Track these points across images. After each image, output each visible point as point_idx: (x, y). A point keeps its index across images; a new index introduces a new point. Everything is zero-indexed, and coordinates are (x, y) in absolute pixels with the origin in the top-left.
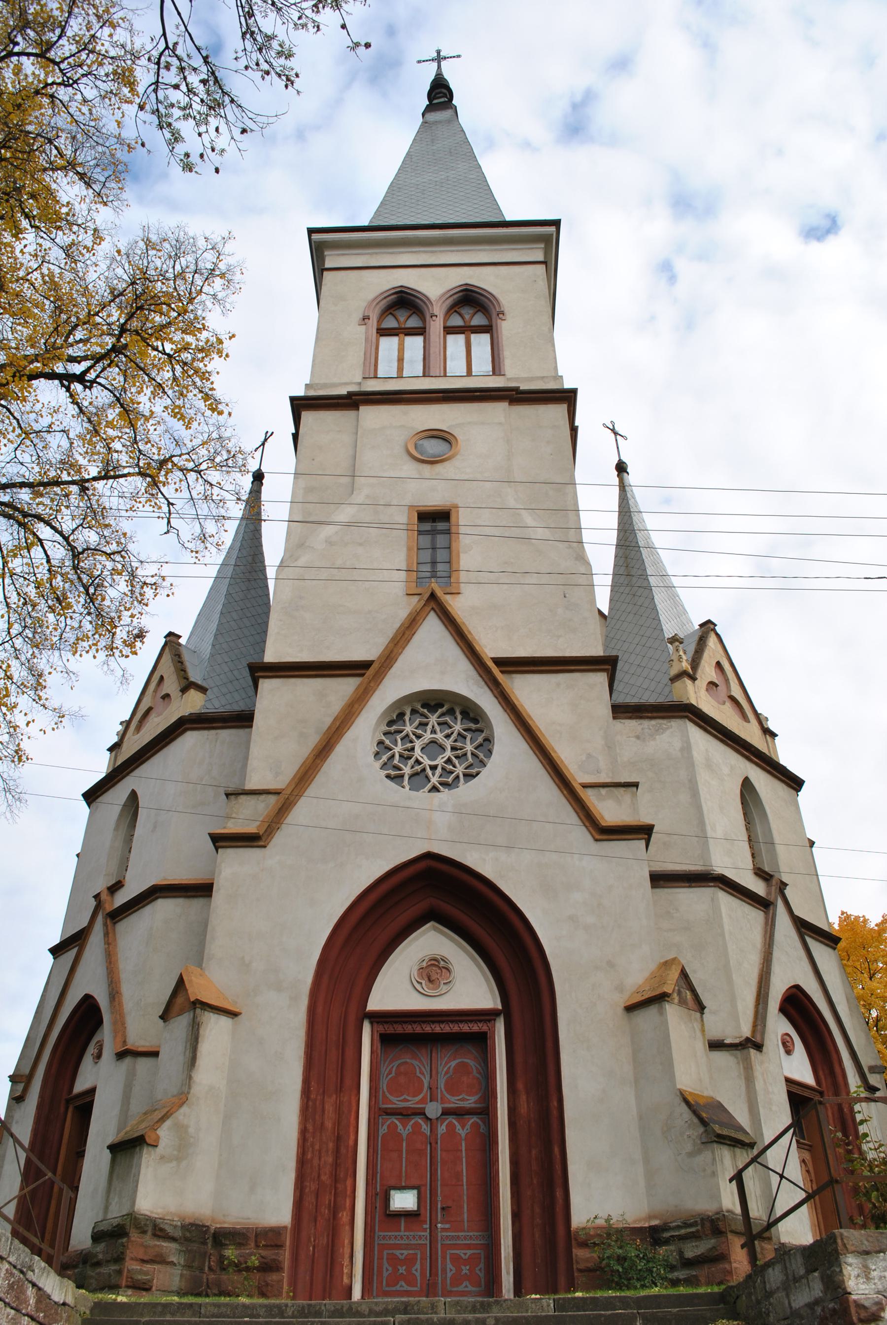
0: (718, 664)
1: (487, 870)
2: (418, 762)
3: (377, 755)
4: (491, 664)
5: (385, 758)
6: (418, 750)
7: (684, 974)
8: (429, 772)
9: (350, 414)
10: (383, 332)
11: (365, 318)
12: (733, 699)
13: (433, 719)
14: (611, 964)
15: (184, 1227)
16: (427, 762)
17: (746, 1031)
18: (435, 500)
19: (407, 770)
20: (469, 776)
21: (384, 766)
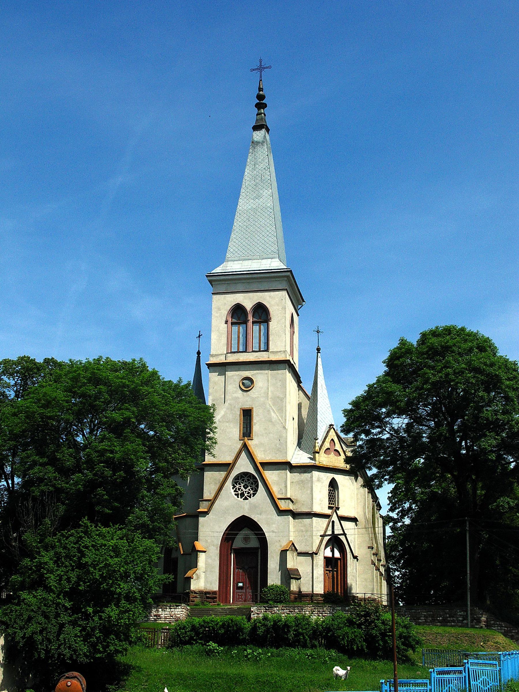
0: (332, 440)
1: (255, 520)
2: (242, 490)
3: (233, 488)
4: (259, 465)
5: (234, 489)
6: (242, 487)
7: (293, 544)
8: (245, 493)
9: (223, 368)
10: (233, 324)
11: (226, 322)
12: (336, 451)
13: (246, 478)
14: (279, 541)
15: (199, 591)
16: (244, 490)
17: (315, 550)
18: (247, 406)
19: (240, 492)
20: (254, 495)
21: (235, 491)
